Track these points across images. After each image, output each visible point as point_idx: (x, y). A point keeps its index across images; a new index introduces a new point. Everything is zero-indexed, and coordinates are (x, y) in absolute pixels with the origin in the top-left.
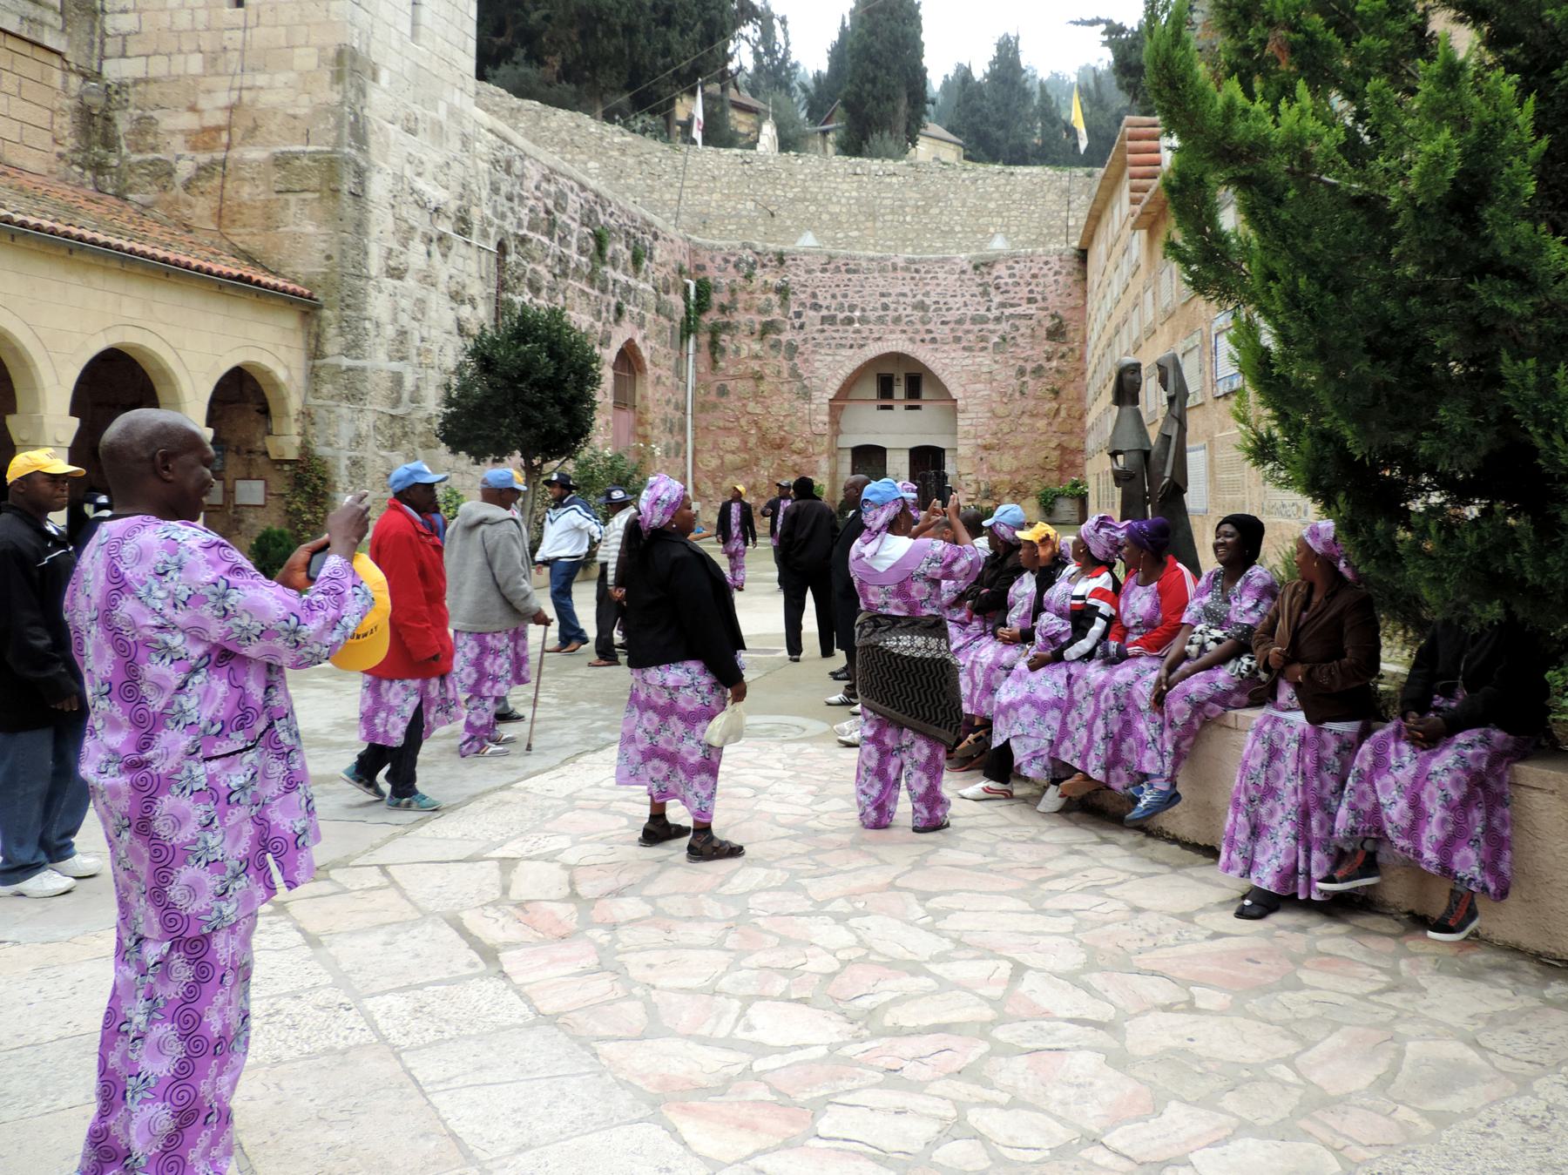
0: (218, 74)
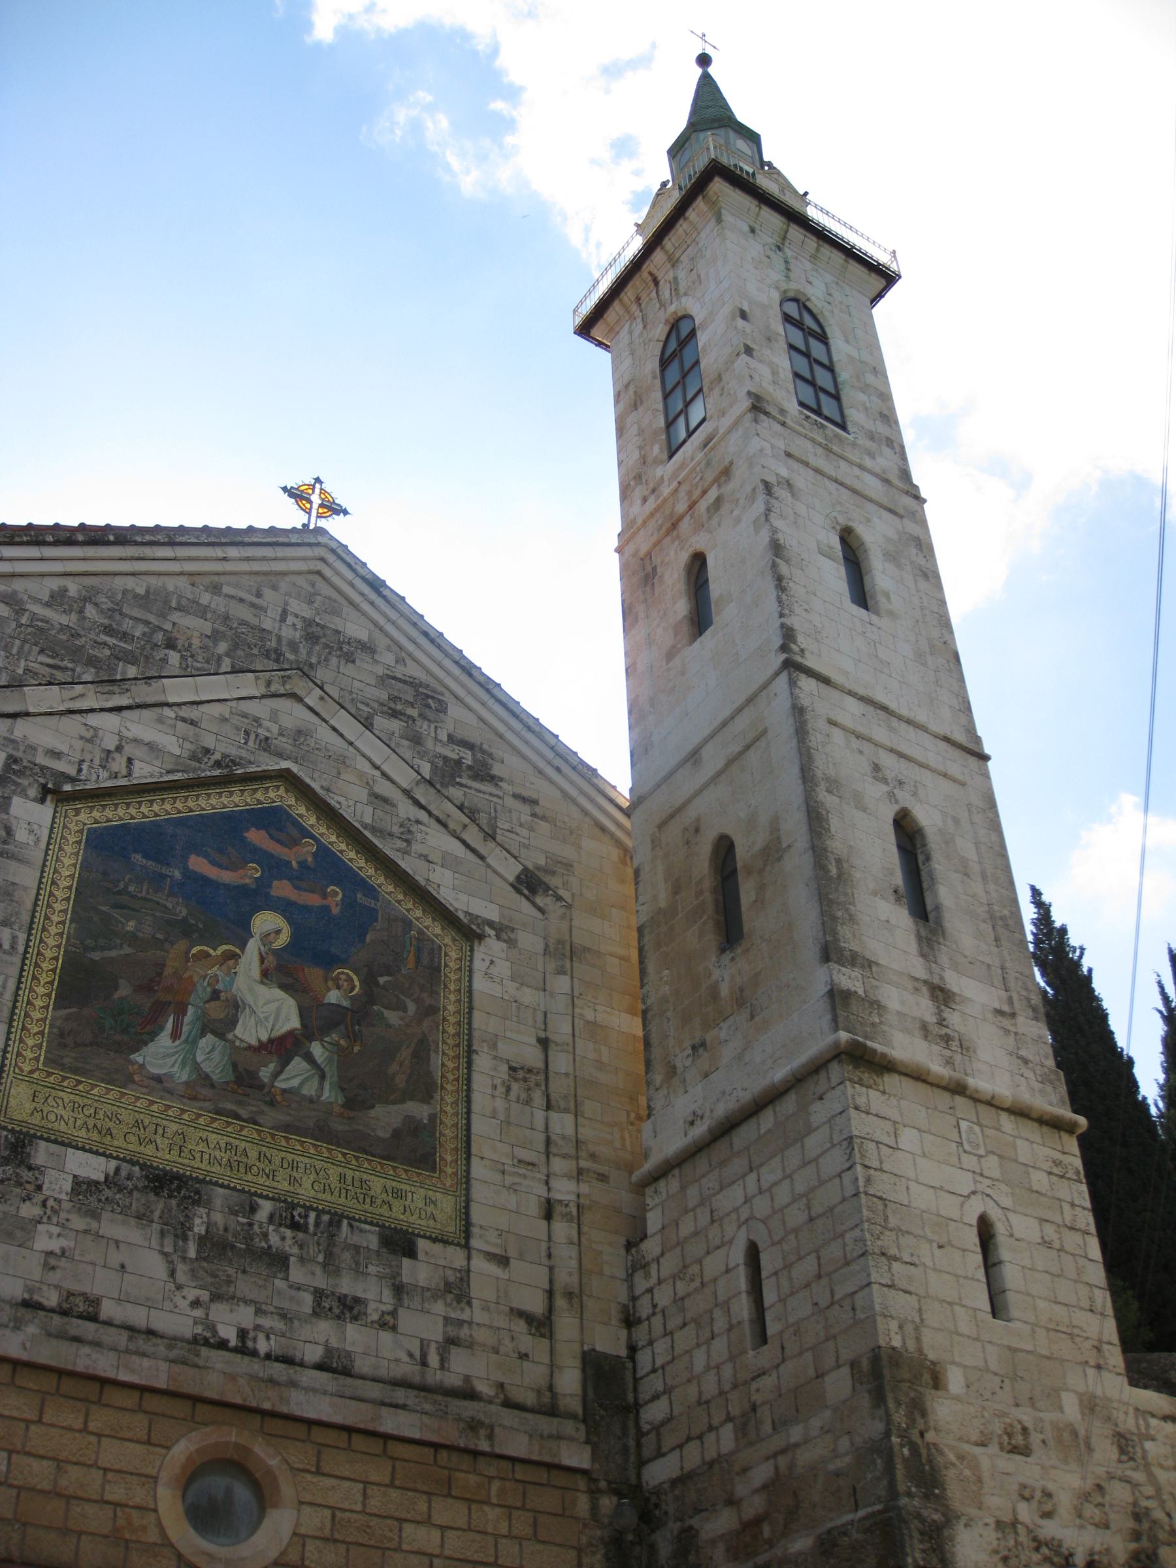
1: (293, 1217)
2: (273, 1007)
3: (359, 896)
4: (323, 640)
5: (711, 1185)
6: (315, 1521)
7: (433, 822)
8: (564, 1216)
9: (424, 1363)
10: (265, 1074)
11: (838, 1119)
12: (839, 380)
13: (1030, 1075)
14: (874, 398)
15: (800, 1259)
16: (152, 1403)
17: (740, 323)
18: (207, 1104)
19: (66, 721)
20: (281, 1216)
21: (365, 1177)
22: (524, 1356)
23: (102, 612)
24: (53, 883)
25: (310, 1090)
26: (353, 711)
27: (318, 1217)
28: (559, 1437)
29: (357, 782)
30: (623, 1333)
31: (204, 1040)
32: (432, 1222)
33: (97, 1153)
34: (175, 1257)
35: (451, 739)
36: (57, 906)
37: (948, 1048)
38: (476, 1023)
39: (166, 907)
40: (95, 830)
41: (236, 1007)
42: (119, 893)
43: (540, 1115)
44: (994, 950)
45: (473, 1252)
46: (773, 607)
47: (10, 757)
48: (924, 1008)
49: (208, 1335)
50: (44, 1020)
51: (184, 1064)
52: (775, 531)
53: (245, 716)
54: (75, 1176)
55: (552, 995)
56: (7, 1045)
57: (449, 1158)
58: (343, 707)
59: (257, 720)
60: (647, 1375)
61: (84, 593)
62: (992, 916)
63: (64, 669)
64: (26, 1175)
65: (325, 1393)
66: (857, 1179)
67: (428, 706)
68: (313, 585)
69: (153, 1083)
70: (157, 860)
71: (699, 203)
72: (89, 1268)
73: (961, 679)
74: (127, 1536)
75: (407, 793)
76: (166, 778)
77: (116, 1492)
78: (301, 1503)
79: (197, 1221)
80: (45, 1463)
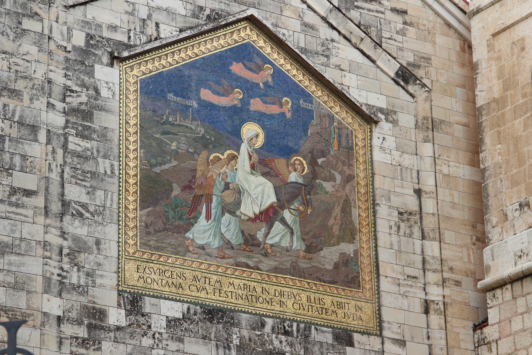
1: (284, 327)
2: (260, 189)
3: (301, 102)
7: (341, 38)
8: (436, 311)
10: (260, 235)
18: (231, 261)
20: (278, 327)
21: (321, 296)
24: (127, 123)
25: (285, 243)
27: (298, 326)
29: (294, 16)
31: (224, 218)
32: (360, 322)
33: (176, 300)
36: (132, 139)
38: (377, 184)
39: (192, 129)
41: (239, 192)
42: (164, 124)
43: (418, 243)
45: (385, 339)
47: (88, 35)
50: (135, 218)
51: (215, 236)
54: (167, 317)
55: (421, 157)
57: (367, 279)
64: (142, 320)
69: (200, 251)
70: (183, 97)
75: (324, 19)
79: (235, 337)
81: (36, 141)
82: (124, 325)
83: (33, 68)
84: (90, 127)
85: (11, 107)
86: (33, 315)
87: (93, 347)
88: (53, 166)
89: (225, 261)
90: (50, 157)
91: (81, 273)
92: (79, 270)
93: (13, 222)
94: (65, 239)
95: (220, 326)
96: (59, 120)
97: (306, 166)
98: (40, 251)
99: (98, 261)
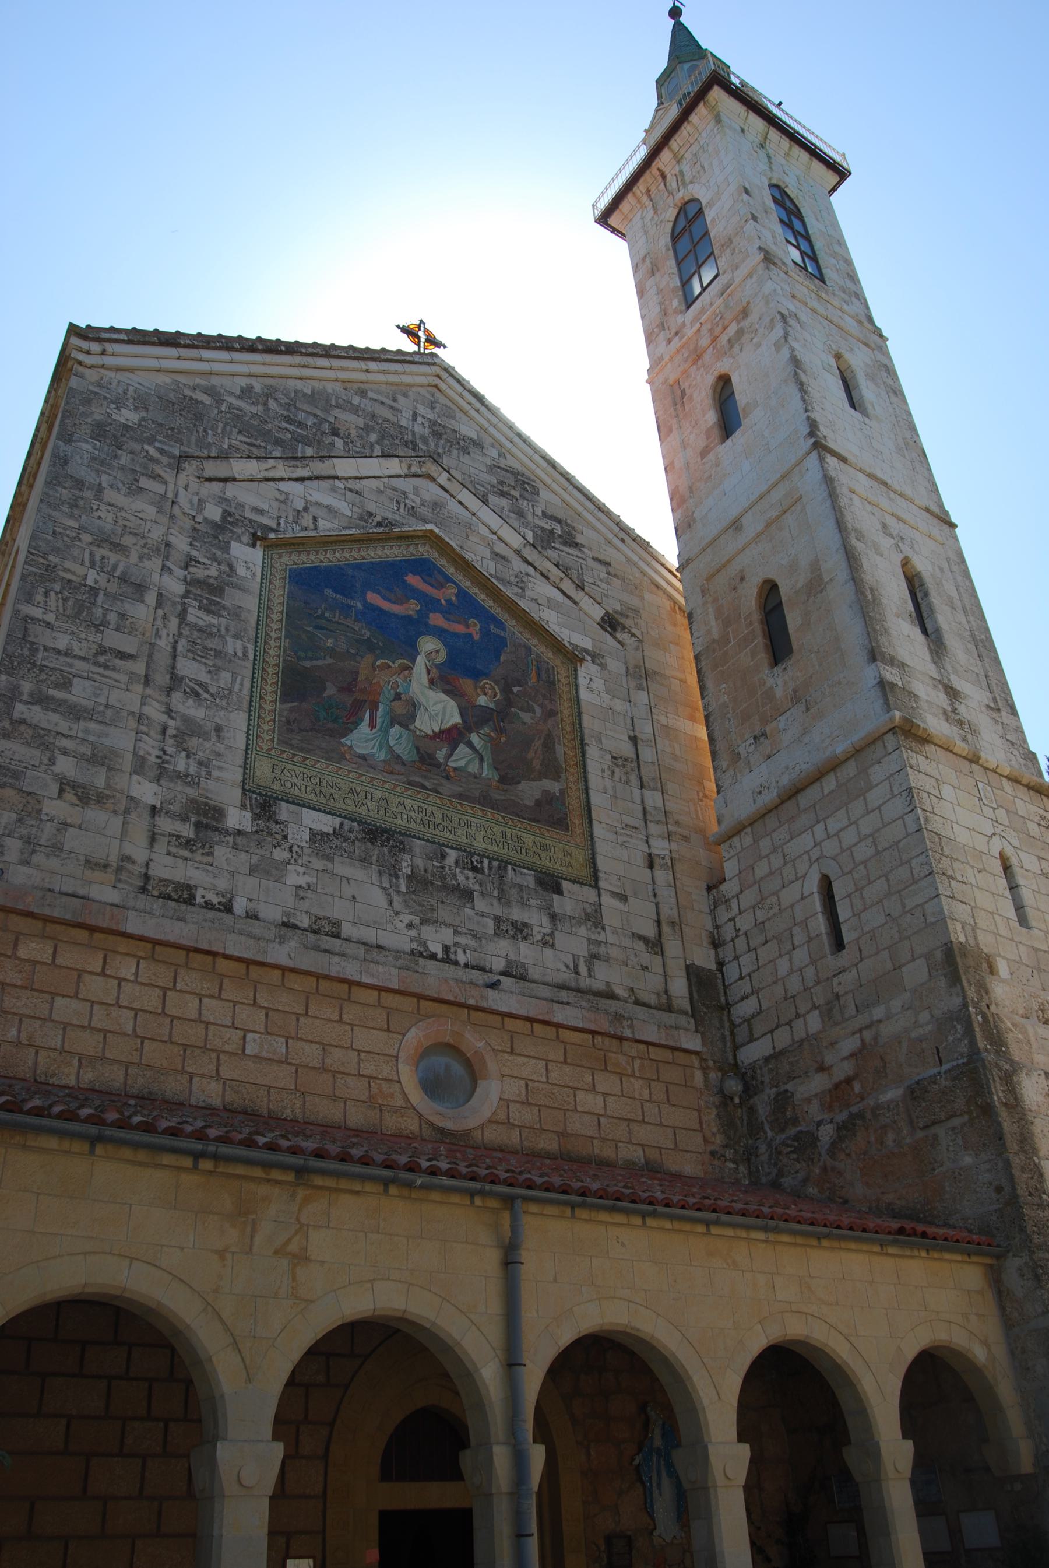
0: (837, 1024)
1: (472, 862)
2: (440, 707)
3: (492, 627)
4: (445, 436)
5: (782, 837)
6: (513, 1089)
8: (662, 866)
9: (577, 973)
10: (440, 755)
11: (896, 776)
12: (816, 248)
13: (1015, 752)
14: (841, 262)
15: (870, 883)
16: (388, 999)
17: (745, 197)
19: (264, 485)
22: (645, 968)
23: (281, 405)
24: (269, 608)
25: (473, 768)
26: (473, 490)
27: (490, 863)
28: (677, 1028)
30: (712, 952)
33: (325, 812)
34: (391, 891)
35: (544, 514)
36: (274, 626)
37: (962, 729)
40: (295, 570)
41: (413, 706)
43: (637, 792)
44: (979, 663)
46: (800, 404)
47: (225, 511)
48: (942, 699)
49: (422, 949)
51: (381, 747)
52: (793, 350)
53: (395, 490)
55: (635, 704)
56: (249, 729)
57: (577, 822)
58: (465, 487)
59: (404, 493)
60: (736, 982)
61: (266, 390)
62: (974, 639)
63: (259, 447)
64: (275, 828)
65: (512, 992)
66: (919, 819)
67: (525, 489)
68: (433, 395)
69: (361, 761)
70: (344, 595)
71: (701, 109)
72: (330, 899)
73: (929, 469)
74: (380, 1102)
75: (518, 552)
76: (344, 532)
77: (368, 1068)
78: (503, 1076)
79: (404, 864)
80: (315, 1047)
81: (143, 601)
82: (249, 829)
83: (148, 527)
84: (218, 603)
85: (112, 561)
86: (114, 797)
87: (201, 851)
88: (163, 633)
89: (391, 776)
90: (159, 622)
91: (191, 761)
92: (188, 757)
93: (97, 684)
94: (172, 718)
95: (386, 850)
96: (175, 586)
97: (498, 691)
98: (132, 723)
99: (217, 750)
